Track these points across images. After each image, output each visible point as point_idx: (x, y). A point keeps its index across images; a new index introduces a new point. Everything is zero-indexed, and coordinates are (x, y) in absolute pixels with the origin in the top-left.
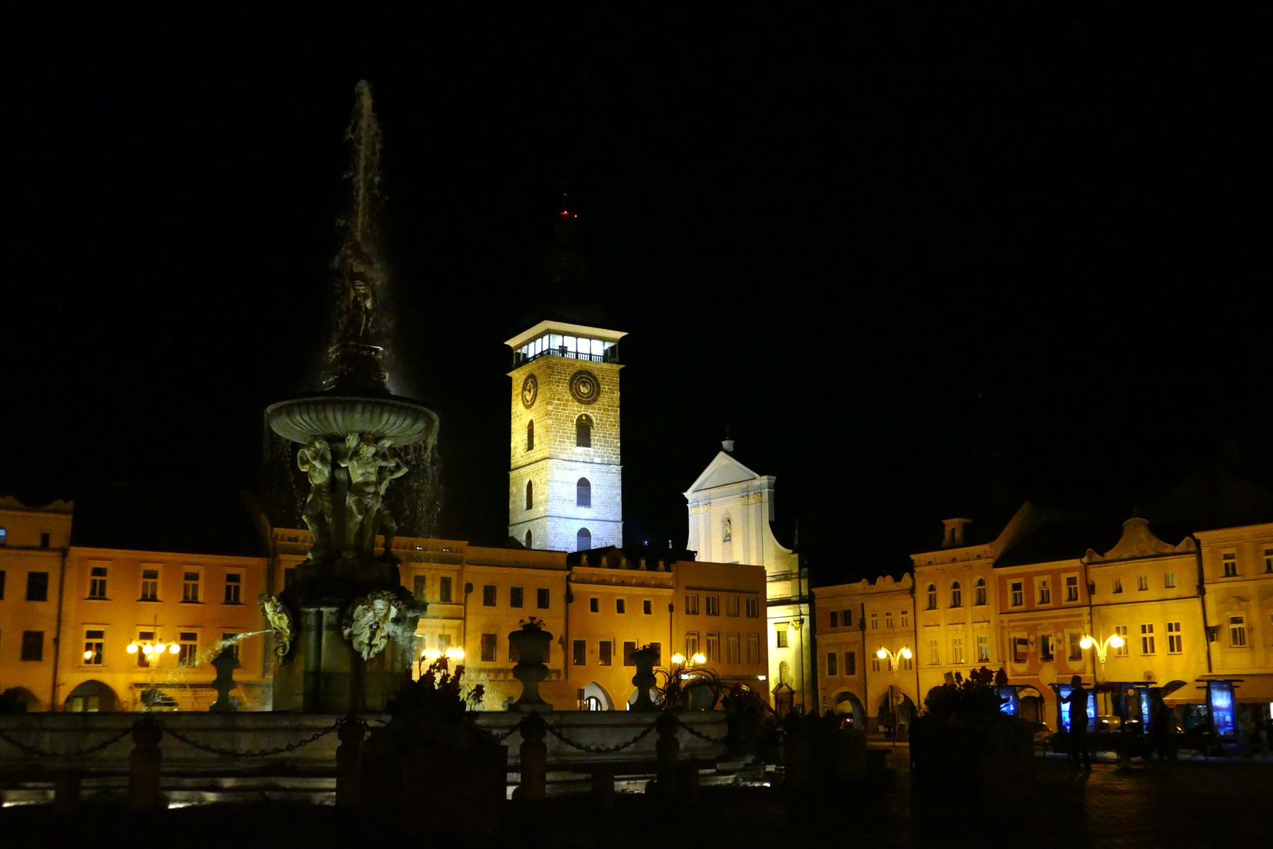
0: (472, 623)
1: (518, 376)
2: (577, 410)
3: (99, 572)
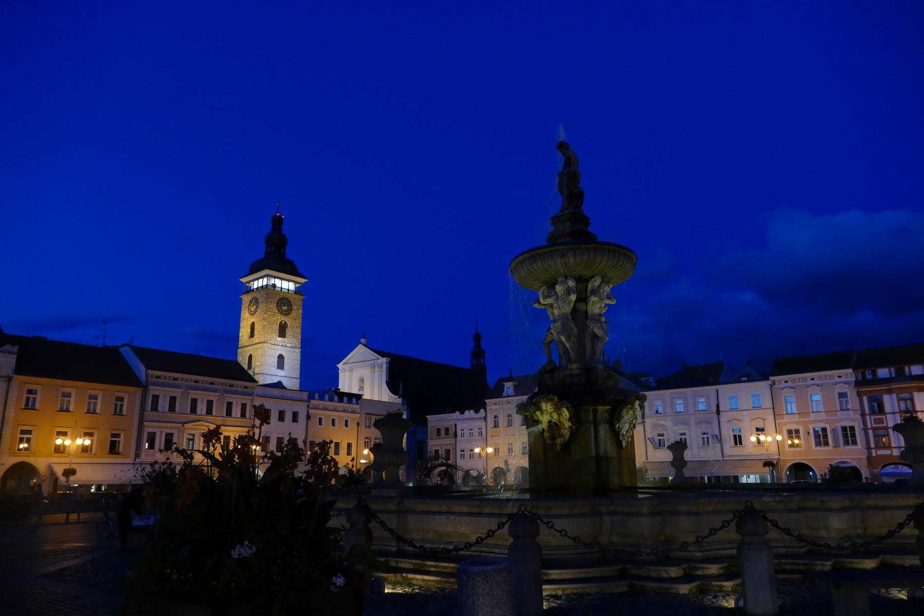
1: (246, 299)
2: (280, 318)
3: (30, 392)
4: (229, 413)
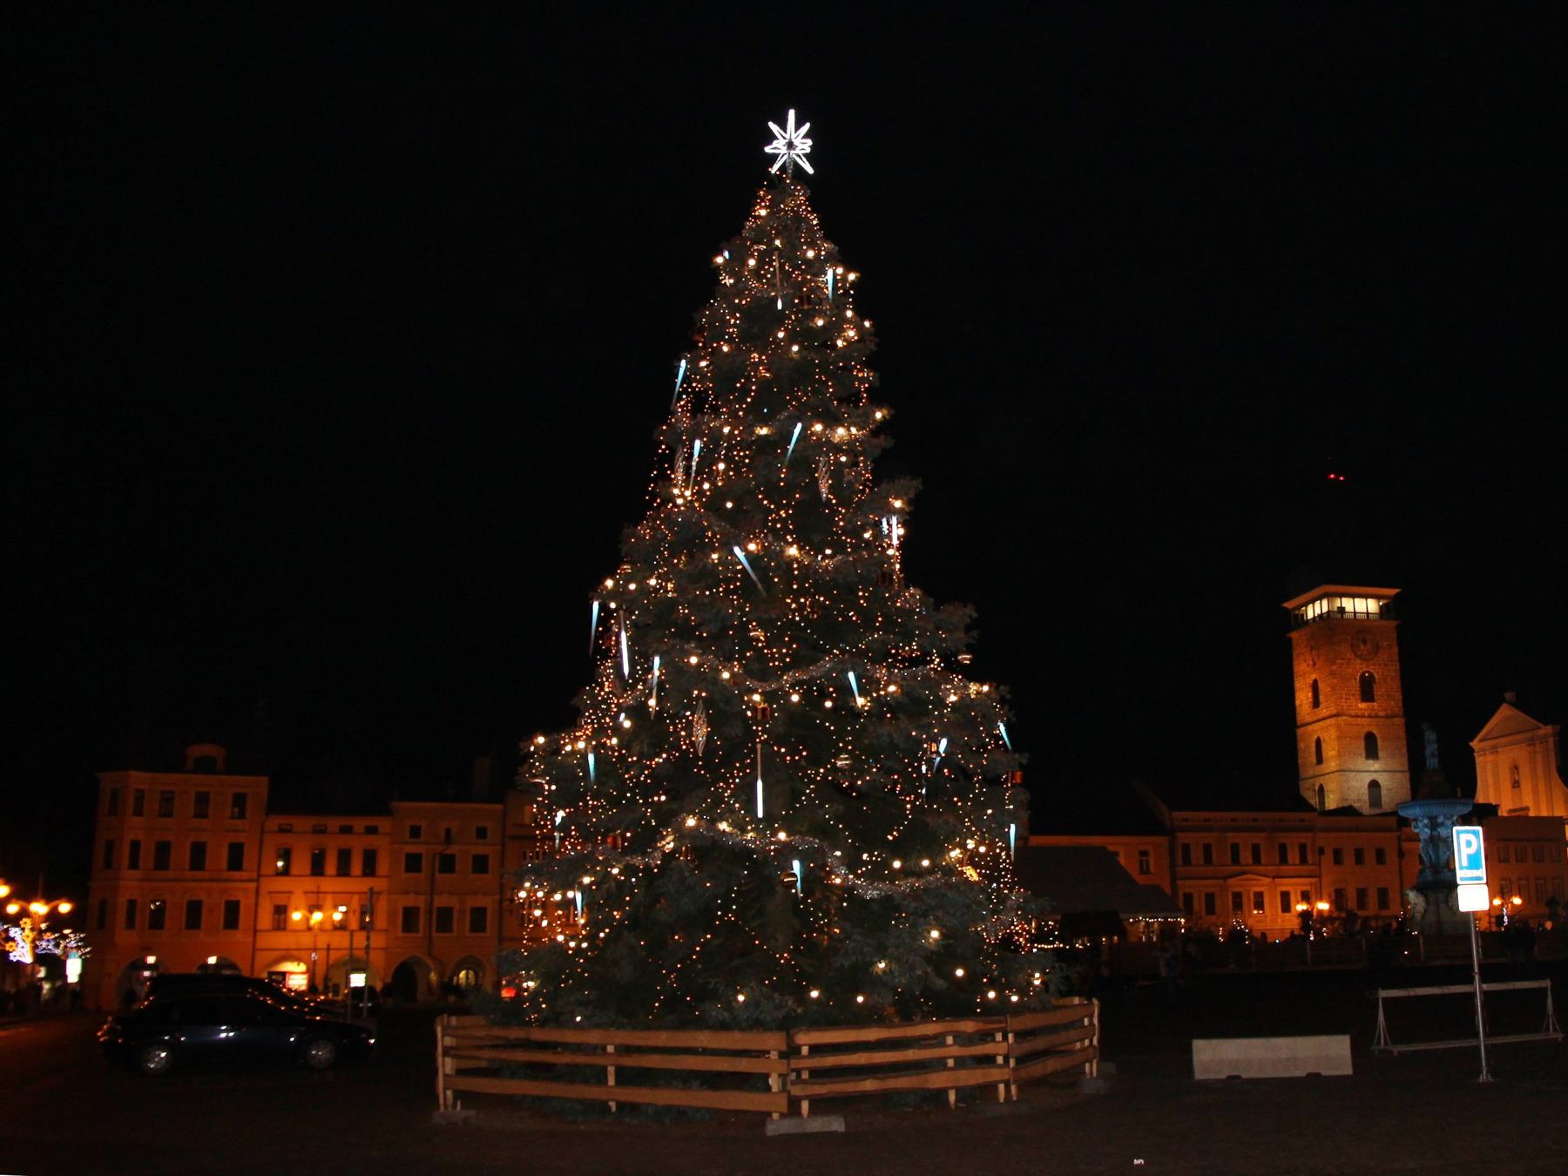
0: (1325, 881)
2: (1358, 668)
4: (1284, 860)
